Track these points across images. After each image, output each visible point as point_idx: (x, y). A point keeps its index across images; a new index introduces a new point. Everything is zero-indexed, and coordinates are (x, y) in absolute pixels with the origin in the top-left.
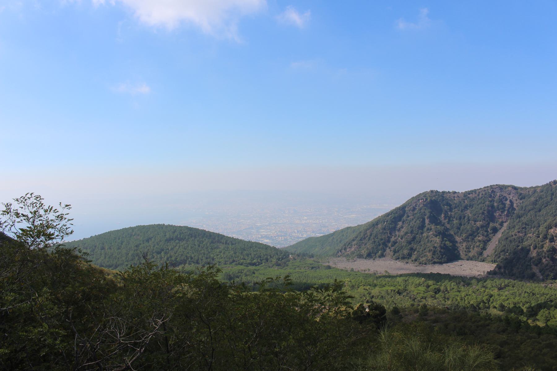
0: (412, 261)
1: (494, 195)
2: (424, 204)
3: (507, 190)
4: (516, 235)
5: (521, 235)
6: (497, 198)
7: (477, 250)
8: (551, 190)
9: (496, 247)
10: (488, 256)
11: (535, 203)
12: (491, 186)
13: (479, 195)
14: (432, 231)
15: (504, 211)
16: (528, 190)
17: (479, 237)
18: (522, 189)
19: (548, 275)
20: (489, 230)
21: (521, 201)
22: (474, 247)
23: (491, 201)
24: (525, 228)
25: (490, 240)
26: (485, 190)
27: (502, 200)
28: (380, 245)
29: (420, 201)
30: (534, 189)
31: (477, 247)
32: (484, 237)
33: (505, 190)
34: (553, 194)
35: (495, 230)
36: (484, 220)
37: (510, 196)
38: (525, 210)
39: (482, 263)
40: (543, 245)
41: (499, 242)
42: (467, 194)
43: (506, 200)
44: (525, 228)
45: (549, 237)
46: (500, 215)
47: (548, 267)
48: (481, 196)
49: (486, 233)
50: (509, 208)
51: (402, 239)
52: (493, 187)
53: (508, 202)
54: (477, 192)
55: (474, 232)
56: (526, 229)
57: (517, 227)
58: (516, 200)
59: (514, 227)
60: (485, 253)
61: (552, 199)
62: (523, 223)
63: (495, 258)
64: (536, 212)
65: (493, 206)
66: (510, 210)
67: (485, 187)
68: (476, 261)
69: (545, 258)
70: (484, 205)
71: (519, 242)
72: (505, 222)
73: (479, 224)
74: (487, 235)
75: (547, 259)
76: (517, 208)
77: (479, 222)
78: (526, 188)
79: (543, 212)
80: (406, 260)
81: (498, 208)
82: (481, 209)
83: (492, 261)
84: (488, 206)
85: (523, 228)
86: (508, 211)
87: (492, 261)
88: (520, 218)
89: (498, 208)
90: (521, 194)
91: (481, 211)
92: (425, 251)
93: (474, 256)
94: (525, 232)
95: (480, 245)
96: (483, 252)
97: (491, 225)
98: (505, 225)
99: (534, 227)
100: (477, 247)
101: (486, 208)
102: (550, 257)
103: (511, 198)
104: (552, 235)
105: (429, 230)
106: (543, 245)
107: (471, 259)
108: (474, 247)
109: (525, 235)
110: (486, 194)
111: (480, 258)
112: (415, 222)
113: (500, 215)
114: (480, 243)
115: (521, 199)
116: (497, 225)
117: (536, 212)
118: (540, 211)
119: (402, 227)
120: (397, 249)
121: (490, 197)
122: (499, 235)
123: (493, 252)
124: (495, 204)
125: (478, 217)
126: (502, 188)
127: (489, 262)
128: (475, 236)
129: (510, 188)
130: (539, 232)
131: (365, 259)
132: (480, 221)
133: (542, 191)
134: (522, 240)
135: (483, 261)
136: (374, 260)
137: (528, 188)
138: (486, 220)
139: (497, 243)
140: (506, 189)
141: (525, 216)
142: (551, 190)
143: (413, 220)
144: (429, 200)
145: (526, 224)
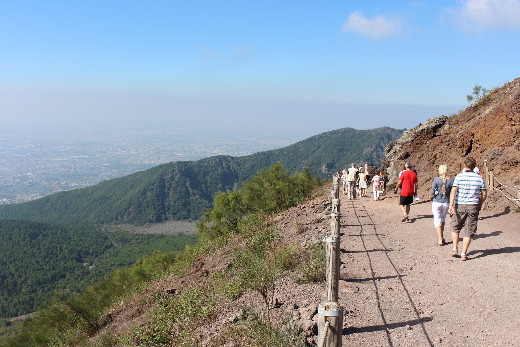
0: (193, 219)
2: (180, 174)
12: (217, 156)
14: (197, 195)
18: (236, 158)
21: (239, 168)
28: (159, 210)
29: (177, 171)
38: (246, 174)
42: (201, 162)
51: (175, 203)
58: (236, 167)
80: (188, 220)
92: (199, 211)
105: (194, 194)
112: (181, 189)
119: (169, 194)
120: (175, 211)
126: (225, 158)
129: (230, 158)
131: (155, 223)
136: (163, 223)
143: (177, 187)
144: (183, 170)
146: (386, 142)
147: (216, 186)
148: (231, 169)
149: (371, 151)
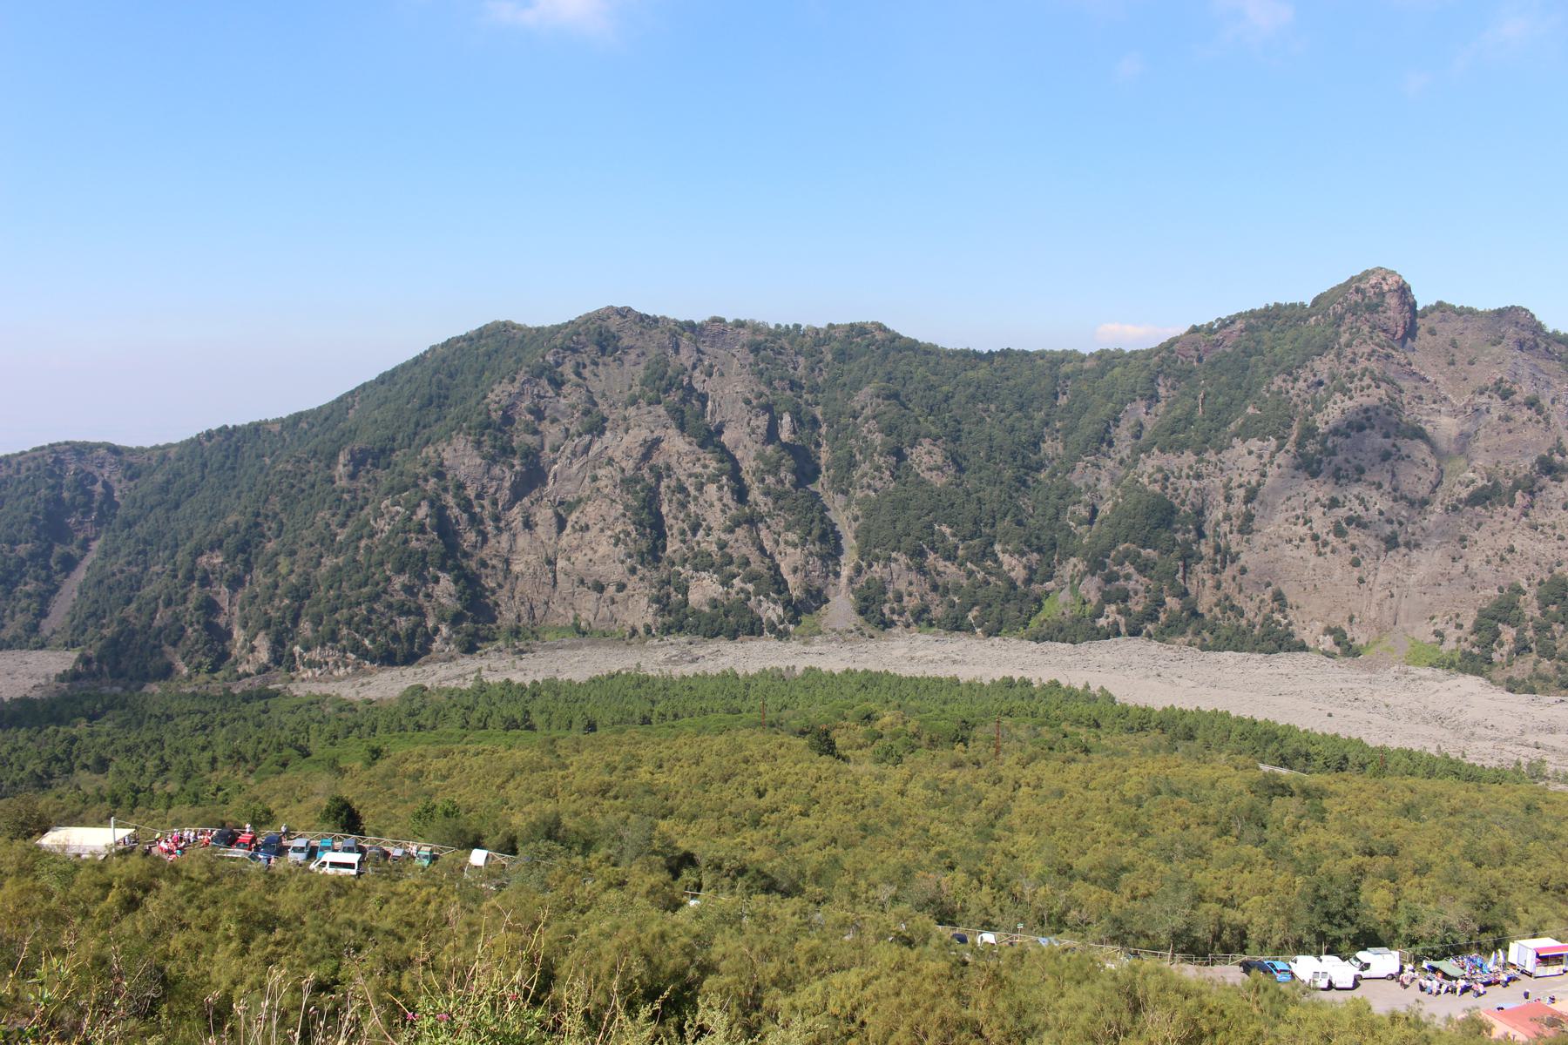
1: (61, 469)
3: (95, 455)
4: (122, 571)
5: (135, 569)
6: (69, 477)
7: (22, 619)
8: (201, 456)
9: (74, 607)
10: (54, 632)
11: (165, 488)
12: (51, 445)
13: (18, 471)
15: (91, 510)
16: (146, 455)
17: (25, 584)
18: (131, 451)
19: (200, 665)
20: (52, 563)
21: (132, 484)
22: (13, 613)
23: (53, 488)
24: (143, 554)
25: (57, 588)
26: (35, 458)
27: (84, 482)
30: (163, 453)
31: (22, 611)
32: (41, 584)
33: (89, 457)
34: (205, 465)
35: (69, 564)
36: (37, 538)
37: (103, 471)
38: (141, 507)
39: (40, 653)
40: (185, 594)
41: (81, 593)
43: (94, 481)
44: (144, 552)
45: (198, 574)
46: (81, 523)
47: (200, 646)
48: (24, 474)
49: (43, 574)
50: (102, 504)
52: (57, 448)
53: (98, 488)
54: (14, 463)
55: (11, 573)
56: (146, 555)
57: (124, 551)
58: (120, 482)
59: (117, 551)
60: (47, 626)
61: (203, 478)
62: (138, 541)
63: (72, 635)
64: (168, 510)
65: (59, 501)
66: (105, 507)
67: (35, 450)
68: (21, 648)
69: (191, 625)
70: (36, 498)
71: (132, 588)
72: (94, 539)
73: (23, 550)
74: (48, 579)
75: (196, 627)
76: (122, 502)
77: (23, 545)
78: (142, 450)
79: (186, 509)
81: (73, 504)
82: (27, 509)
83: (66, 644)
84: (47, 501)
85: (139, 553)
86: (100, 509)
87: (66, 644)
88: (130, 526)
89: (73, 504)
90: (130, 466)
91: (27, 516)
93: (15, 638)
94: (145, 562)
95: (29, 605)
96: (38, 623)
97: (58, 549)
98: (95, 545)
99: (166, 548)
100: (22, 611)
101: (41, 506)
102: (202, 621)
103: (106, 475)
104: (205, 571)
106: (185, 594)
107: (9, 647)
108: (13, 613)
109: (146, 569)
110: (38, 468)
111: (33, 640)
113: (81, 523)
114: (29, 601)
115: (131, 478)
116: (74, 549)
117: (168, 510)
118: (177, 506)
121: (50, 477)
122: (80, 574)
123: (68, 619)
124: (66, 495)
125: (20, 531)
126: (81, 450)
127: (57, 647)
128: (16, 584)
129: (102, 452)
130: (175, 564)
132: (27, 542)
133: (181, 459)
134: (139, 582)
135: (42, 646)
137: (147, 450)
138: (43, 537)
139: (76, 595)
140: (91, 453)
141: (143, 522)
142: (201, 456)
145: (146, 542)
146: (587, 362)
147: (12, 551)
148: (98, 488)
149: (510, 395)
